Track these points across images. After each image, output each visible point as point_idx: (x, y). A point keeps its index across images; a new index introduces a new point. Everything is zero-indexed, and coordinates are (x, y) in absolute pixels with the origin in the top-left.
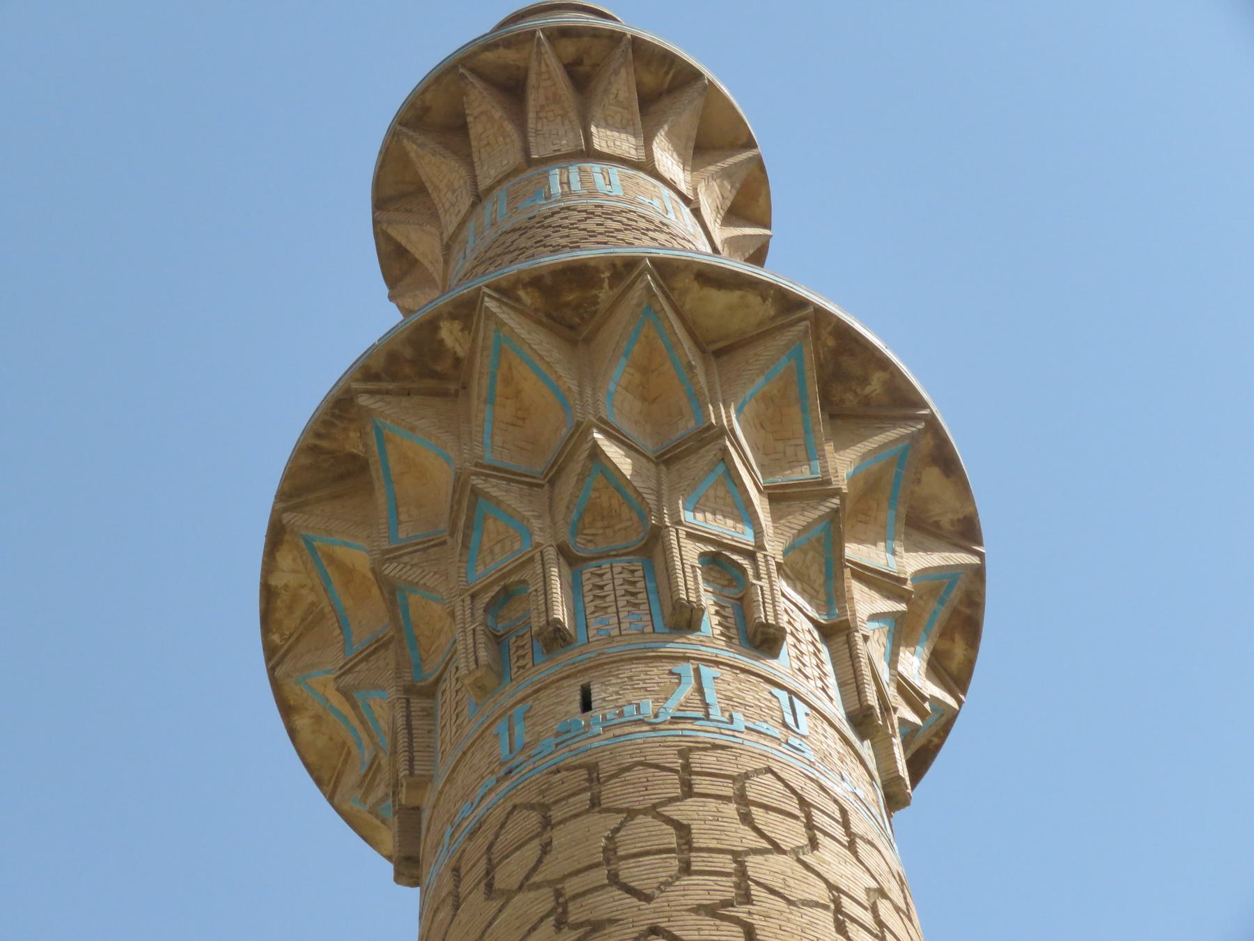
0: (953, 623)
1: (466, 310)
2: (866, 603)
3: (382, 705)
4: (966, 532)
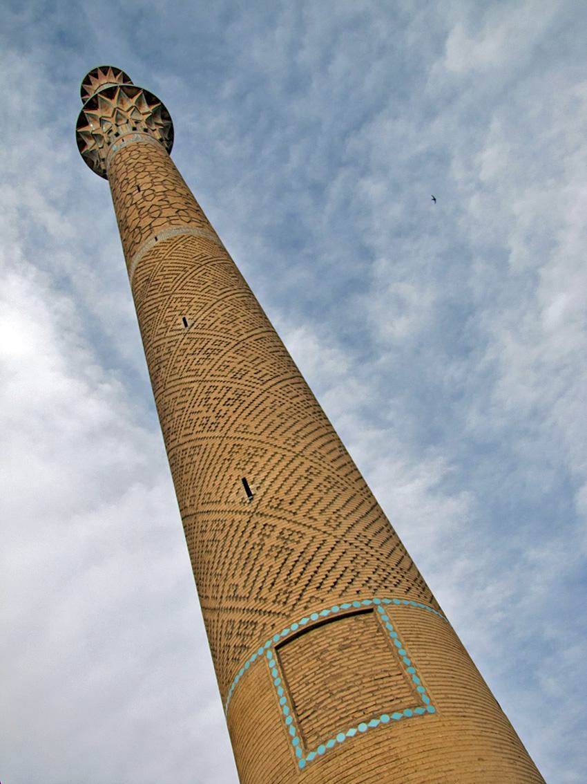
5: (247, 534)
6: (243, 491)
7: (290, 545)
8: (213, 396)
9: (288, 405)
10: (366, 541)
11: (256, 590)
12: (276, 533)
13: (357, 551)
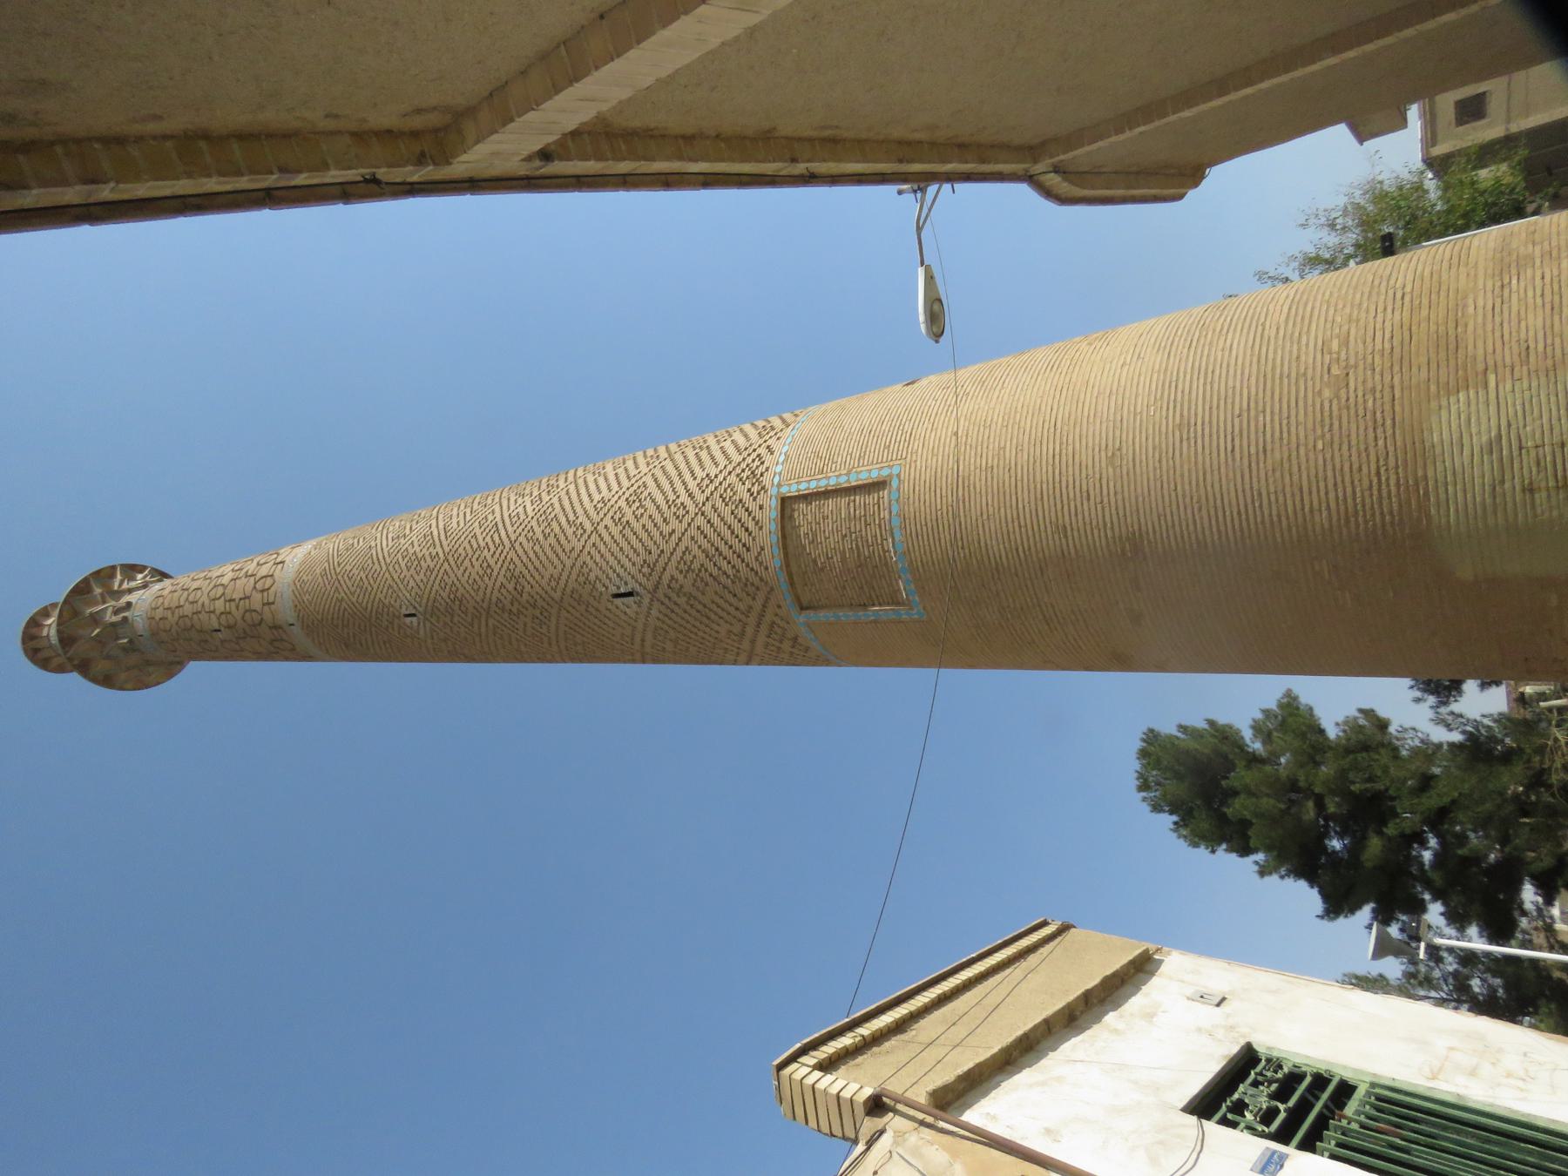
0: (131, 570)
1: (70, 659)
2: (125, 586)
3: (151, 669)
4: (113, 568)
5: (676, 609)
6: (625, 600)
7: (696, 566)
8: (508, 606)
9: (534, 523)
10: (706, 481)
11: (738, 614)
12: (680, 577)
13: (716, 495)
